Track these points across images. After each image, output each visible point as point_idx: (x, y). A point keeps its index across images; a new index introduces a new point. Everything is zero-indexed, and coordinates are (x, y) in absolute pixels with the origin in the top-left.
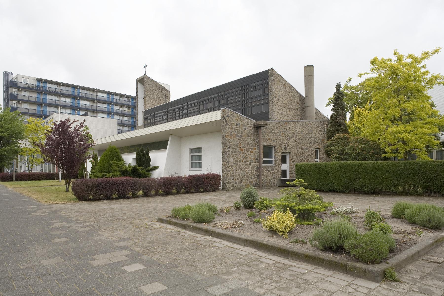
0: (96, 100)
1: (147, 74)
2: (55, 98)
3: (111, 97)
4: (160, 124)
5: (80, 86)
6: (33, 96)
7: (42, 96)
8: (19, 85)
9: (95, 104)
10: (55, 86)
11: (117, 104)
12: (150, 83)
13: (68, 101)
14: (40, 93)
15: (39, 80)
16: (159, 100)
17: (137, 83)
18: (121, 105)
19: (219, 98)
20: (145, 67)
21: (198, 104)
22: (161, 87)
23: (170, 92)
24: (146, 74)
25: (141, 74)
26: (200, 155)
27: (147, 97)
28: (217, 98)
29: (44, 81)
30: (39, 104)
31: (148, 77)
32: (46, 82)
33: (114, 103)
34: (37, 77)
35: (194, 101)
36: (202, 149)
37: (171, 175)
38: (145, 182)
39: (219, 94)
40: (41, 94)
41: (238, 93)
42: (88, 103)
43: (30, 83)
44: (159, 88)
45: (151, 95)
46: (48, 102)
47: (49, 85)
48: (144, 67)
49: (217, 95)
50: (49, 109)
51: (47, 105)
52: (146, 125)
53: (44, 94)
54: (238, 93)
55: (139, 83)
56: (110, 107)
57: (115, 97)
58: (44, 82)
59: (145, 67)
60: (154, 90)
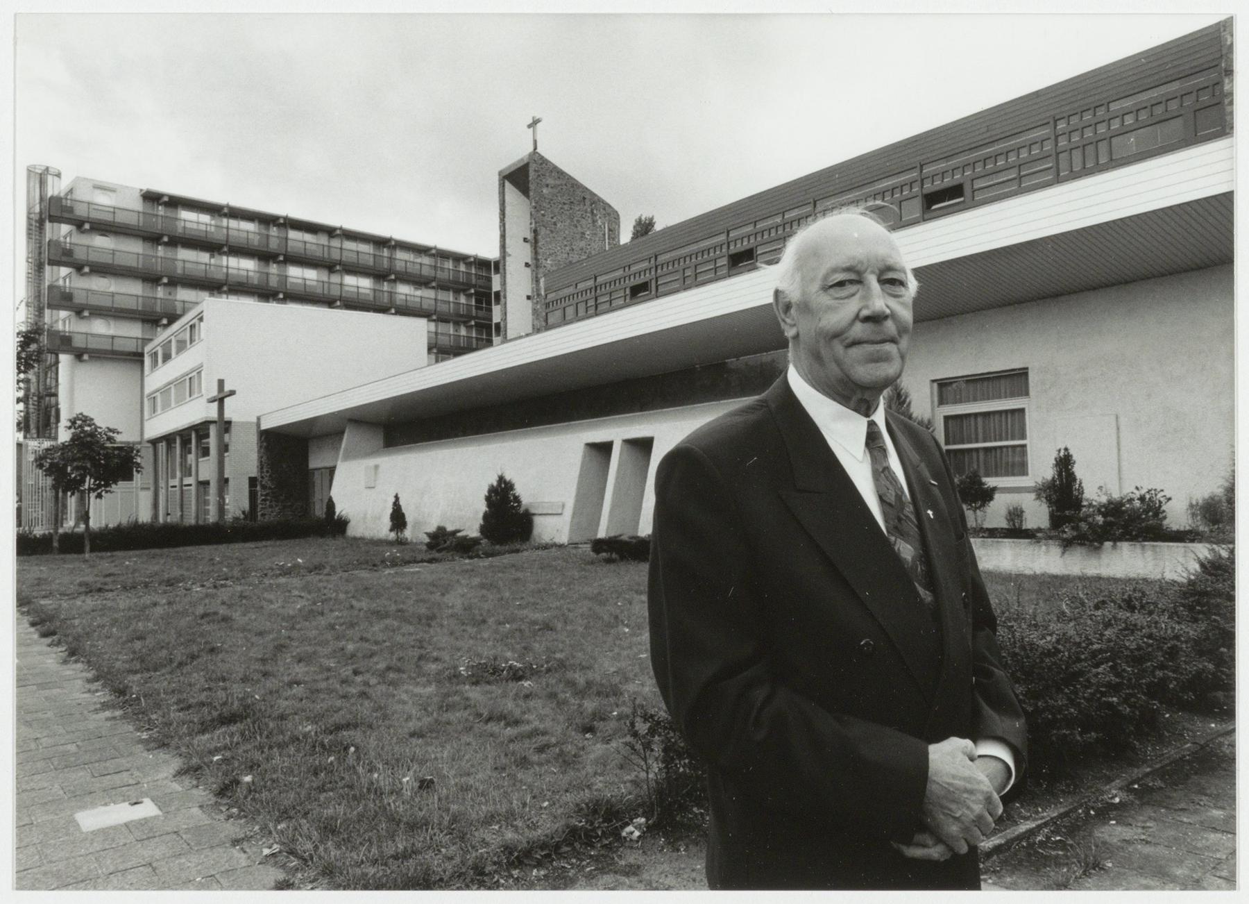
0: (340, 263)
1: (538, 150)
2: (204, 257)
3: (386, 253)
4: (930, 219)
5: (286, 218)
6: (131, 250)
7: (160, 292)
8: (81, 211)
9: (335, 279)
10: (205, 218)
11: (405, 278)
12: (550, 181)
13: (246, 266)
14: (153, 239)
15: (151, 198)
16: (582, 244)
17: (502, 186)
18: (420, 282)
19: (656, 270)
20: (535, 123)
21: (653, 273)
22: (588, 197)
23: (618, 215)
24: (535, 149)
25: (517, 153)
26: (1013, 411)
27: (543, 232)
28: (650, 273)
29: (166, 199)
30: (151, 278)
31: (544, 161)
32: (176, 203)
33: (396, 273)
34: (145, 188)
35: (581, 286)
36: (1033, 378)
37: (1149, 553)
38: (1209, 662)
39: (728, 235)
40: (156, 203)
41: (749, 241)
42: (311, 275)
43: (121, 206)
44: (584, 198)
45: (555, 224)
46: (179, 271)
47: (186, 215)
48: (529, 126)
49: (723, 238)
50: (184, 294)
51: (176, 281)
52: (543, 324)
53: (165, 285)
54: (749, 241)
55: (507, 184)
56: (386, 288)
57: (401, 255)
58: (166, 244)
59: (535, 123)
60: (566, 207)
